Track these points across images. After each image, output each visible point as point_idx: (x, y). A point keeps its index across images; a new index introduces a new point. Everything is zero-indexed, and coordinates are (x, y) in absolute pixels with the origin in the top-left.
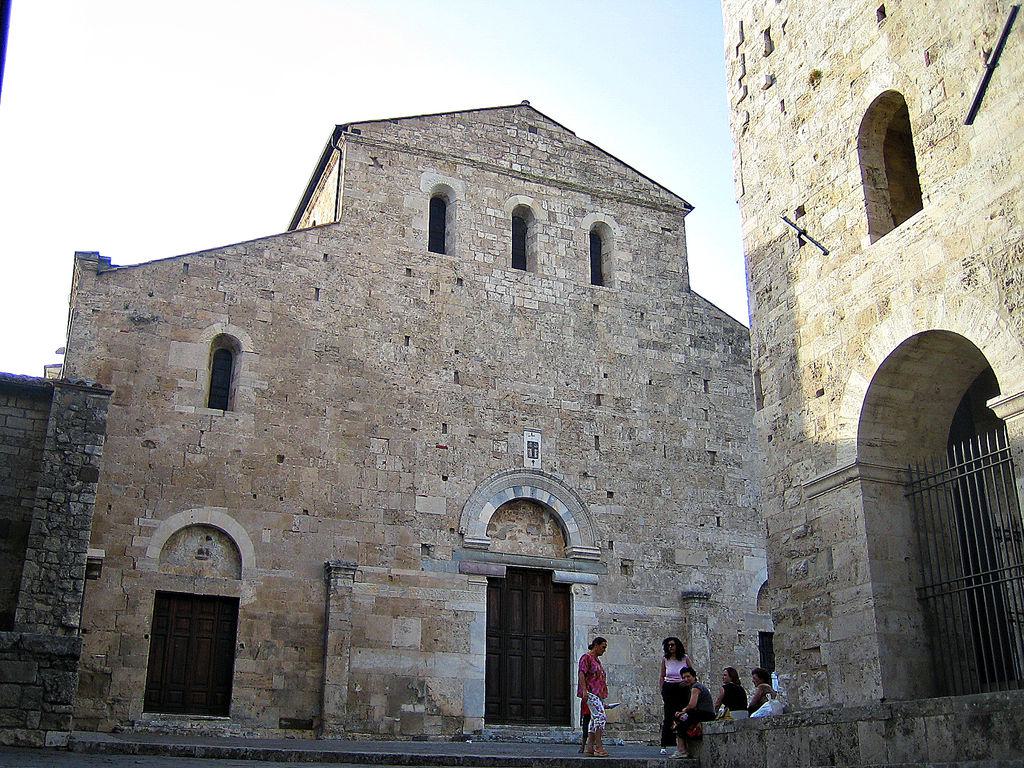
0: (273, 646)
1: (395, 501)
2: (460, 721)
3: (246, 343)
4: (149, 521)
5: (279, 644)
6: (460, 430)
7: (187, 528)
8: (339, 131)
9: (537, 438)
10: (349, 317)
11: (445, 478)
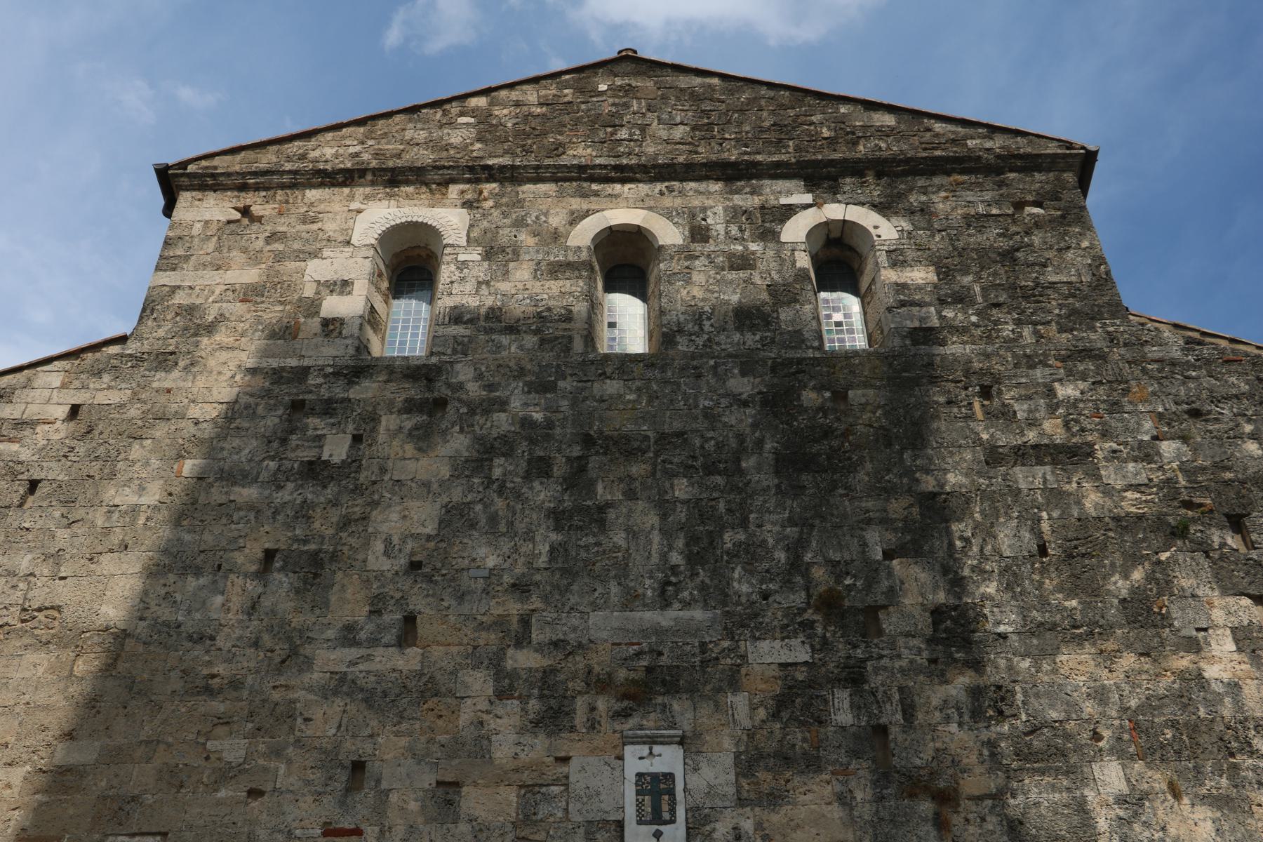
9: (668, 759)
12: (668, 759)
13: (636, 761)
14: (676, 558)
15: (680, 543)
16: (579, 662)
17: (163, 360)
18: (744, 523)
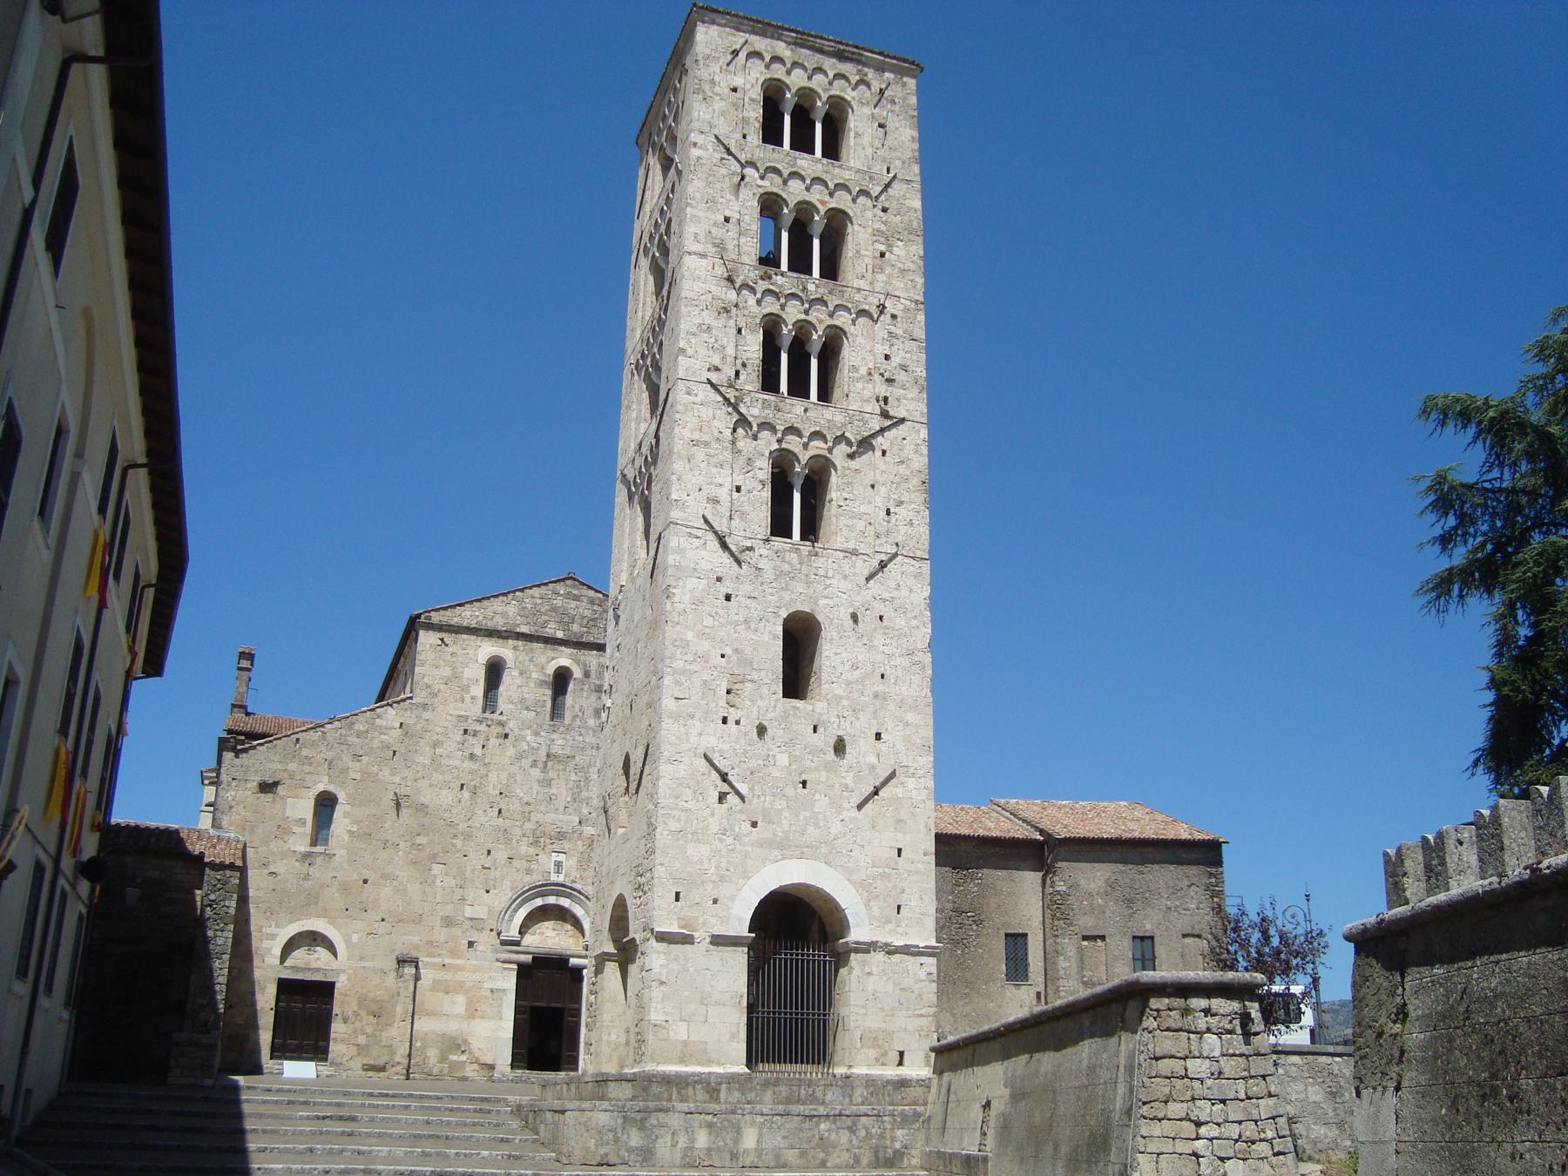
1: (449, 910)
2: (492, 1067)
3: (341, 796)
4: (273, 930)
5: (363, 1013)
6: (500, 854)
12: (562, 857)
13: (555, 857)
17: (424, 706)
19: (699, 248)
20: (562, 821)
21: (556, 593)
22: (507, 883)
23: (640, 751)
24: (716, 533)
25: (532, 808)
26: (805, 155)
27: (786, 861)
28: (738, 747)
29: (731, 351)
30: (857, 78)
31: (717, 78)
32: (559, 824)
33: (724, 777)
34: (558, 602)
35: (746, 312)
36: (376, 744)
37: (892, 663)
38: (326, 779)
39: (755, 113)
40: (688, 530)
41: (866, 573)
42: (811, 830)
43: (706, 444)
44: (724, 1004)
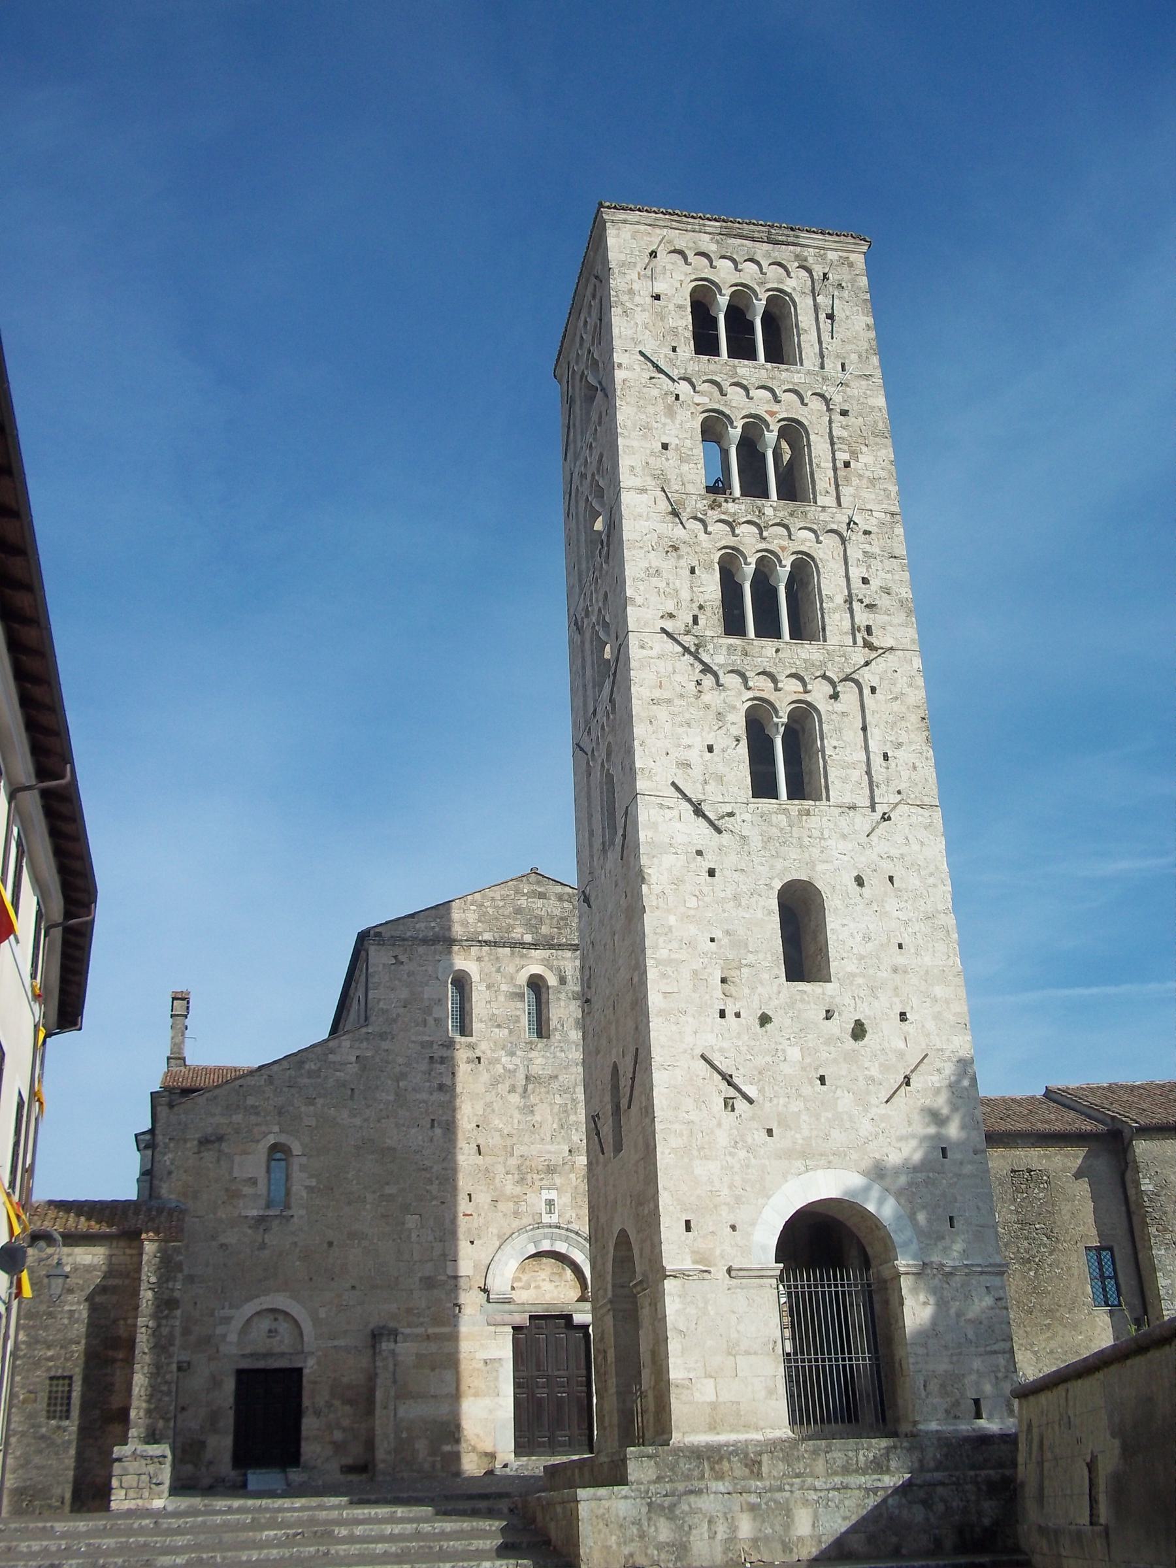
0: (332, 1405)
1: (428, 1269)
2: (492, 1456)
3: (297, 1149)
4: (227, 1312)
5: (337, 1403)
7: (258, 1313)
8: (363, 937)
9: (553, 1195)
10: (381, 1110)
11: (472, 1242)
12: (553, 1195)
13: (546, 1195)
14: (555, 1126)
15: (556, 1120)
16: (528, 1163)
17: (383, 1036)
18: (576, 1113)
19: (637, 482)
20: (550, 1152)
21: (518, 892)
22: (493, 1230)
23: (629, 1059)
24: (689, 801)
25: (514, 1140)
26: (746, 362)
27: (810, 1173)
28: (740, 1043)
29: (685, 594)
30: (796, 264)
31: (636, 287)
32: (547, 1156)
33: (728, 1079)
34: (523, 902)
35: (698, 549)
36: (331, 1082)
37: (910, 930)
38: (276, 1129)
39: (685, 321)
40: (659, 800)
41: (868, 829)
42: (835, 1134)
43: (669, 701)
44: (755, 1353)
